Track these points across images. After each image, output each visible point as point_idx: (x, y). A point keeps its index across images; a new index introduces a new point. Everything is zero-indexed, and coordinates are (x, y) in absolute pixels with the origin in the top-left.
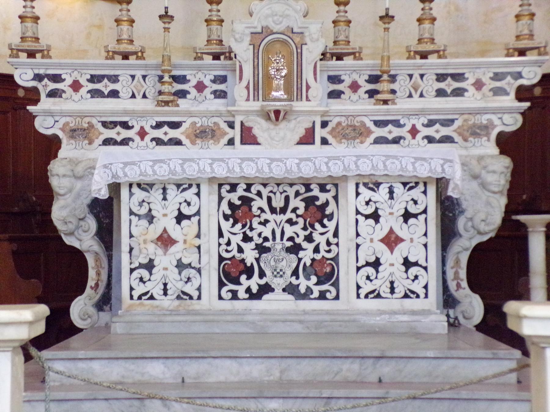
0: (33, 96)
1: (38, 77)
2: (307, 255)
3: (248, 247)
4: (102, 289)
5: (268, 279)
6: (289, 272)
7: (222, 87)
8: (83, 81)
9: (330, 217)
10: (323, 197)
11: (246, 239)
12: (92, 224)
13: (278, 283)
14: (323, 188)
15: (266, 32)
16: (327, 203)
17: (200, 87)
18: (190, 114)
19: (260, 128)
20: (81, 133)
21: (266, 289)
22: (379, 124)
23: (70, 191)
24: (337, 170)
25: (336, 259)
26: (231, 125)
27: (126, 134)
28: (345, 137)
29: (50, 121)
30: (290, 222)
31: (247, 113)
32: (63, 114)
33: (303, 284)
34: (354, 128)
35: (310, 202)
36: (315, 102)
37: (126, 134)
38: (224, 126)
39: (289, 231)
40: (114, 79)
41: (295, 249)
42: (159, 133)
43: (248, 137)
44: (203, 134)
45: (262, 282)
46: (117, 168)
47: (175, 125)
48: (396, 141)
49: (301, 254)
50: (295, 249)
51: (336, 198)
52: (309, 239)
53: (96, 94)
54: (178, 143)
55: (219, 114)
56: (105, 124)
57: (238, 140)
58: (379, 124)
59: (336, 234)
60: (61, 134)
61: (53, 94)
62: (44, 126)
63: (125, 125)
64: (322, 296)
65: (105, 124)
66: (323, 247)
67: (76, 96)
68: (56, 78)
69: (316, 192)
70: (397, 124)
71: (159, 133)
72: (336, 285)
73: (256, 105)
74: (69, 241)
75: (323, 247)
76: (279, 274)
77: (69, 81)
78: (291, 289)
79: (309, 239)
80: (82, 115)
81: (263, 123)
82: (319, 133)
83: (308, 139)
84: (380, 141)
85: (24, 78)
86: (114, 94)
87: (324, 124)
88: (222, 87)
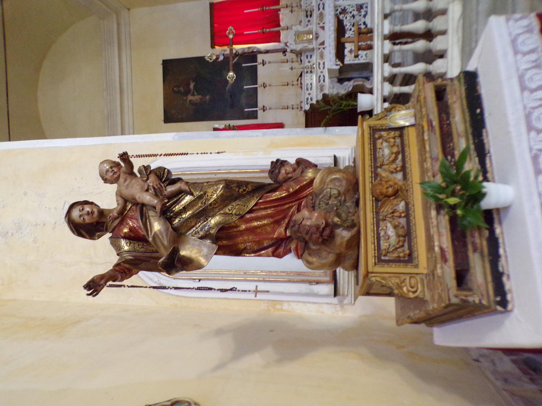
0: (312, 105)
1: (307, 104)
2: (355, 13)
3: (353, 29)
4: (364, 80)
5: (361, 22)
6: (360, 17)
7: (309, 57)
8: (308, 92)
9: (345, 8)
10: (339, 10)
11: (351, 30)
12: (346, 83)
13: (363, 20)
14: (337, 10)
15: (295, 41)
16: (342, 9)
17: (309, 62)
18: (316, 60)
19: (320, 40)
20: (322, 88)
21: (364, 23)
22: (319, 9)
23: (337, 89)
24: (332, 5)
25: (357, 5)
26: (319, 49)
27: (322, 77)
28: (323, 18)
29: (319, 96)
30: (346, 18)
31: (316, 44)
32: (317, 92)
33: (363, 13)
34: (320, 17)
35: (340, 13)
36: (314, 27)
37: (322, 77)
38: (320, 51)
39: (348, 18)
40: (307, 85)
41: (353, 16)
42: (322, 68)
43: (323, 43)
44: (322, 56)
45: (362, 24)
46: (332, 63)
47: (319, 64)
48: (324, 4)
49: (355, 14)
50: (353, 16)
51: (340, 6)
52: (351, 13)
53: (311, 88)
54: (324, 63)
55: (317, 52)
56: (320, 81)
57: (323, 46)
58: (319, 9)
59: (350, 5)
60: (322, 93)
61: (311, 99)
62: (320, 97)
63: (320, 77)
64: (367, 7)
65: (320, 81)
66: (353, 8)
67: (312, 94)
68: (307, 99)
69: (338, 12)
70: (319, 5)
71: (322, 68)
72: (364, 4)
73: (314, 41)
74: (350, 89)
75: (353, 8)
76: (360, 20)
77: (308, 96)
78: (365, 16)
79: (351, 13)
80: (317, 88)
81: (319, 39)
82: (321, 25)
83: (323, 28)
84: (323, 9)
85: (307, 107)
86: (311, 84)
87: (319, 24)
88: (309, 57)
